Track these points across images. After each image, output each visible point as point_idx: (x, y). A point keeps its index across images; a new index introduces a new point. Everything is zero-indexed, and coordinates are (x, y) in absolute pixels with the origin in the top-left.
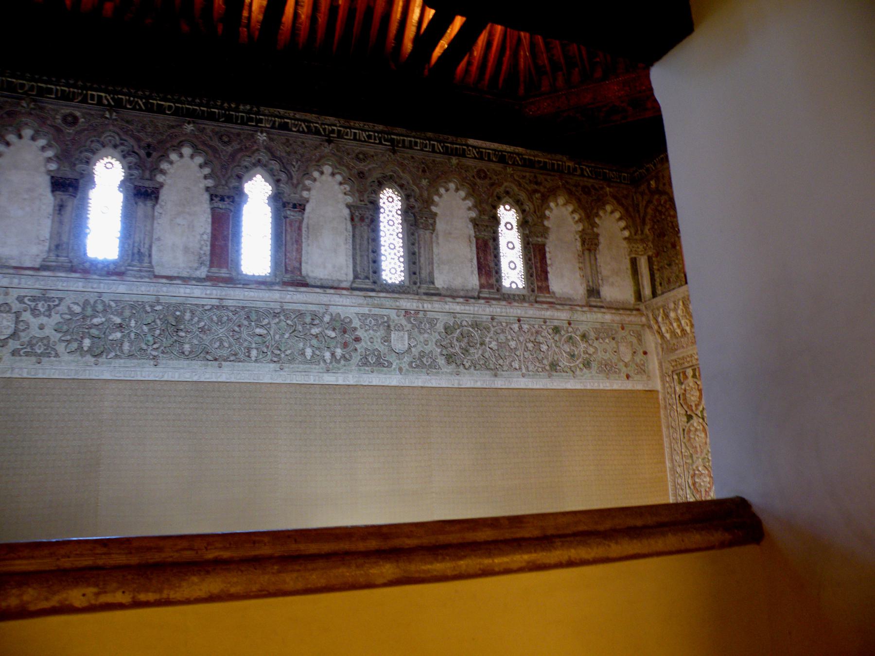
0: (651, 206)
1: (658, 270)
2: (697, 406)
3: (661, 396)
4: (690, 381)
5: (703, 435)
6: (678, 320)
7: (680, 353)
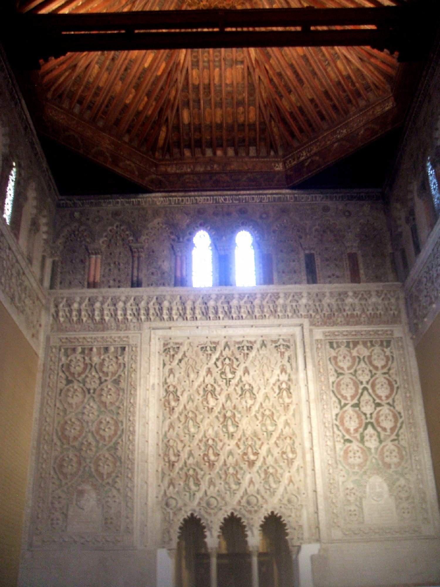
0: (69, 228)
1: (61, 273)
2: (79, 375)
3: (41, 362)
4: (79, 357)
5: (81, 396)
6: (79, 311)
7: (71, 335)
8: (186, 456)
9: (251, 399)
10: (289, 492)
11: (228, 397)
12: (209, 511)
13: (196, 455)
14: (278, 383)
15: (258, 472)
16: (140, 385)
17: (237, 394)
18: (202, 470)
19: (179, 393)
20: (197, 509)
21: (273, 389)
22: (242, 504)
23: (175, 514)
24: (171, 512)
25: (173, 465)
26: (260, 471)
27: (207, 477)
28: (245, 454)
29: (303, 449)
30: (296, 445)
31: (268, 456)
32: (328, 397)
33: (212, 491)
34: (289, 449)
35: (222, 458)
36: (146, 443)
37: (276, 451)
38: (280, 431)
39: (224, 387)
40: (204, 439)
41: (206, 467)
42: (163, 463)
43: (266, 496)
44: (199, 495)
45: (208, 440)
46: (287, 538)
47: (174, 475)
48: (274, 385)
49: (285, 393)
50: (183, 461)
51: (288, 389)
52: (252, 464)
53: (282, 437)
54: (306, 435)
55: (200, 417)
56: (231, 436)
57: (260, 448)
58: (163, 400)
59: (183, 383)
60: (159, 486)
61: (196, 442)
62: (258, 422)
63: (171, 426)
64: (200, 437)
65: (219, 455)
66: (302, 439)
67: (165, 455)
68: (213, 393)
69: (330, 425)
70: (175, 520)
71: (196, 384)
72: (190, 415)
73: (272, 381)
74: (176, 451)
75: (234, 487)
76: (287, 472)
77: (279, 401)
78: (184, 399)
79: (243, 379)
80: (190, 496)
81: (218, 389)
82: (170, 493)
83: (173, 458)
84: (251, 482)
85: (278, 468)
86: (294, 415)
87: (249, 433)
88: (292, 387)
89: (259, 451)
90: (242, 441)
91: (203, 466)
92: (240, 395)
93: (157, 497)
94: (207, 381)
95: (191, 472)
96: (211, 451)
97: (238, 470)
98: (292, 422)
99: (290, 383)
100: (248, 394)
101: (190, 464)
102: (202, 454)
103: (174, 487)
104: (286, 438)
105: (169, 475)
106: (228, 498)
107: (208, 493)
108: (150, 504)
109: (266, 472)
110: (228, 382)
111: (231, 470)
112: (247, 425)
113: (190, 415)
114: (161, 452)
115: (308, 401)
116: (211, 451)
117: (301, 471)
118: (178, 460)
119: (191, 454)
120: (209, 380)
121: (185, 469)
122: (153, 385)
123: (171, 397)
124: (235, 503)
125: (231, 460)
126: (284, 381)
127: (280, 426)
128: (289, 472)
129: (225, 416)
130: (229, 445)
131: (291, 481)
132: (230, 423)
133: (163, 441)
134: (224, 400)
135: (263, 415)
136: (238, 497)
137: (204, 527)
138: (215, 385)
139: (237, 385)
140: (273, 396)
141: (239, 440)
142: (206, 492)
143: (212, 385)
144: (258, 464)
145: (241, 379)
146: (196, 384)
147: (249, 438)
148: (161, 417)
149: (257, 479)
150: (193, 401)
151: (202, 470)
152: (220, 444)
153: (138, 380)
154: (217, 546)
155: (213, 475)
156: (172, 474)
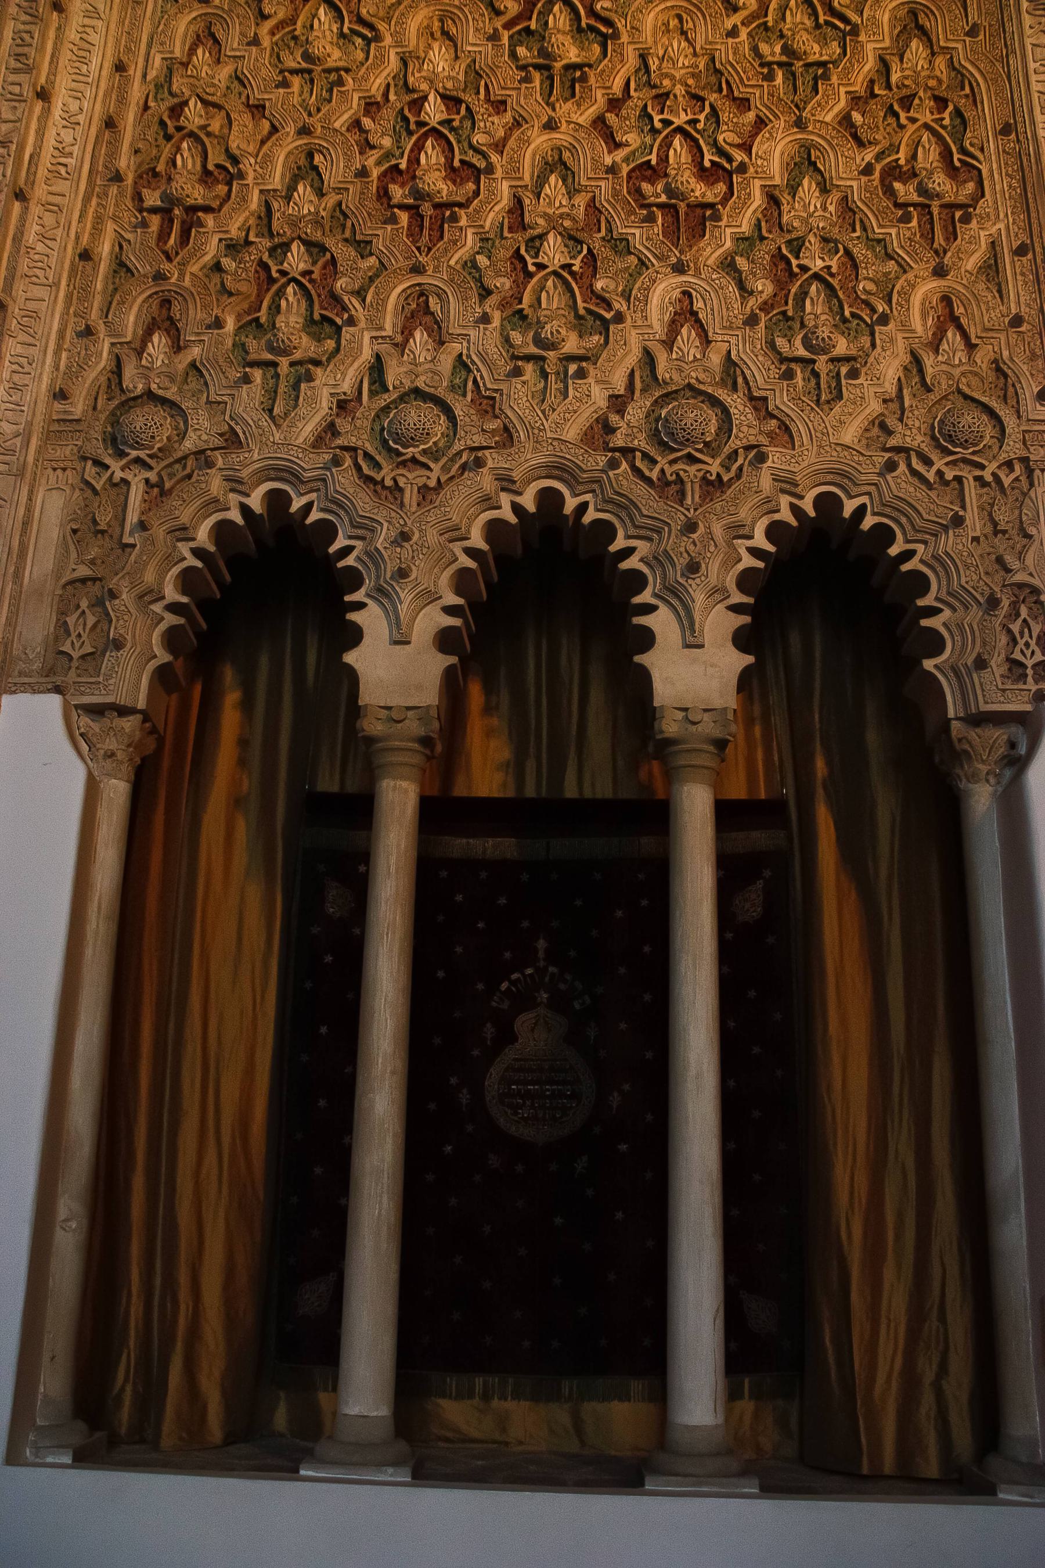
8: (277, 181)
12: (387, 474)
13: (335, 170)
15: (728, 265)
18: (363, 247)
20: (311, 464)
22: (619, 440)
23: (159, 492)
24: (137, 480)
26: (741, 262)
31: (793, 188)
33: (422, 361)
34: (929, 157)
36: (39, 106)
41: (389, 239)
42: (129, 217)
43: (781, 400)
45: (418, 104)
46: (928, 664)
47: (187, 274)
50: (255, 200)
52: (689, 221)
60: (88, 332)
64: (376, 86)
65: (476, 173)
67: (150, 175)
70: (159, 532)
74: (216, 156)
76: (921, 268)
80: (272, 394)
82: (146, 373)
84: (686, 312)
85: (859, 251)
89: (739, 156)
90: (631, 110)
93: (61, 395)
95: (296, 260)
96: (432, 155)
97: (602, 251)
101: (294, 222)
103: (177, 347)
104: (907, 102)
105: (159, 277)
106: (519, 398)
107: (394, 374)
109: (783, 269)
111: (554, 252)
114: (125, 162)
116: (432, 155)
119: (306, 169)
124: (572, 432)
127: (871, 47)
128: (940, 272)
130: (550, 126)
133: (146, 107)
137: (354, 579)
141: (614, 104)
142: (377, 369)
147: (679, 90)
149: (719, 301)
151: (363, 247)
154: (430, 696)
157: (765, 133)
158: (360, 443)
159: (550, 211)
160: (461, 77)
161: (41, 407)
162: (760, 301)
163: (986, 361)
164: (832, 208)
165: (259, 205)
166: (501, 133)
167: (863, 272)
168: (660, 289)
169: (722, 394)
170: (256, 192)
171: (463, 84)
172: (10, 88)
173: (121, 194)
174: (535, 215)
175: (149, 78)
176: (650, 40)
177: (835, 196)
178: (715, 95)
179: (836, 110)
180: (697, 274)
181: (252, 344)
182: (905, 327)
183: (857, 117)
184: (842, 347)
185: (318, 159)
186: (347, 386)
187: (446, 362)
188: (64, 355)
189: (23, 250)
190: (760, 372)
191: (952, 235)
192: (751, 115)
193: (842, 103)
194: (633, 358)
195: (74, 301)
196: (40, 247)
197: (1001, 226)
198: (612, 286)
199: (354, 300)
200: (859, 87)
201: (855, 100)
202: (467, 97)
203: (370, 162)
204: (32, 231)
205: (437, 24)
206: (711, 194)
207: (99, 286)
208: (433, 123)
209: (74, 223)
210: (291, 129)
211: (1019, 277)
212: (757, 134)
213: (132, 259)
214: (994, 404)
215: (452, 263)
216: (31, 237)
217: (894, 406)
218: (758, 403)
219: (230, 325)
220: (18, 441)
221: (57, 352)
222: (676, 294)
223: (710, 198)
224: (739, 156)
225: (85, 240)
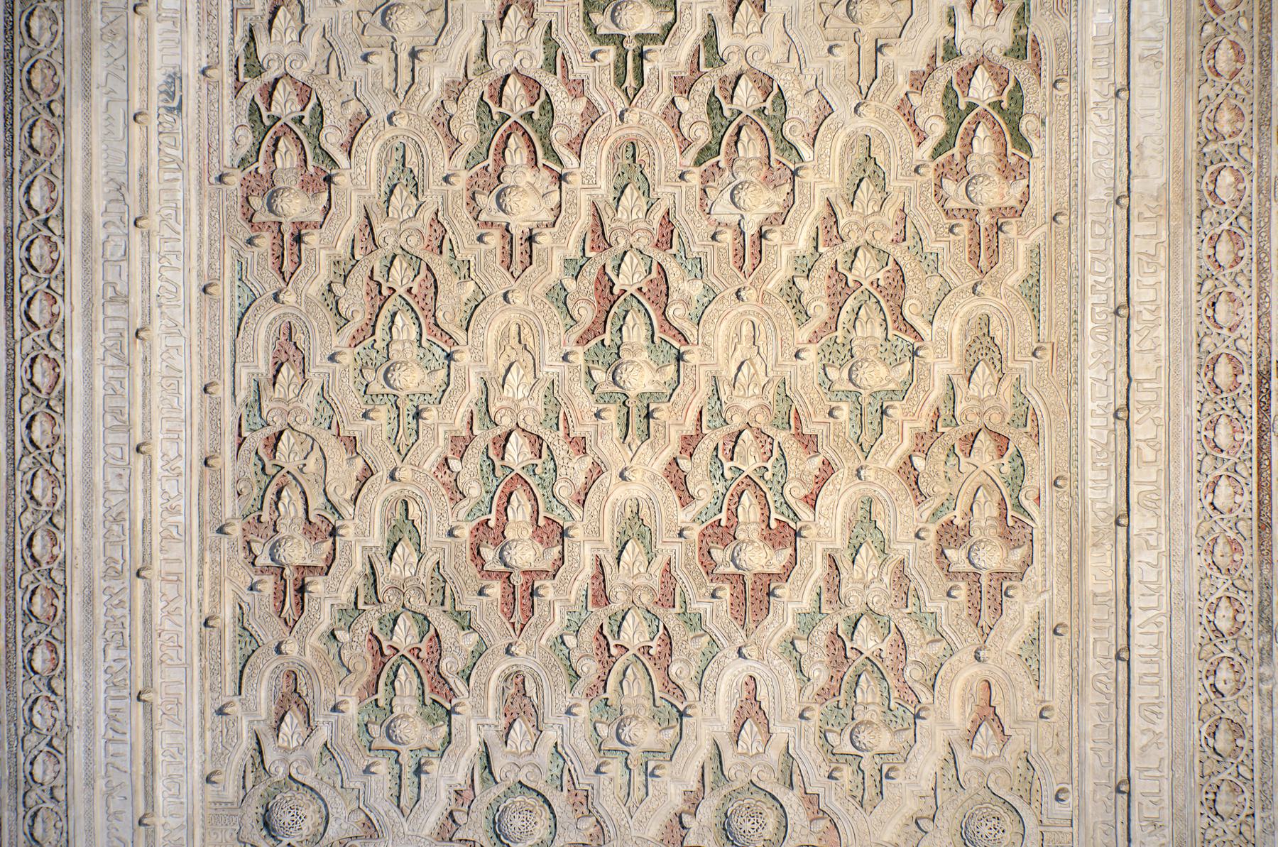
8: (377, 539)
9: (770, 182)
10: (973, 783)
11: (631, 164)
13: (433, 534)
14: (946, 72)
16: (87, 96)
17: (685, 144)
19: (332, 139)
21: (911, 118)
25: (301, 589)
27: (496, 669)
28: (722, 532)
29: (1074, 515)
30: (1037, 479)
32: (1251, 186)
34: (987, 511)
35: (583, 553)
36: (139, 462)
37: (904, 522)
38: (938, 391)
39: (606, 94)
40: (483, 437)
41: (487, 606)
42: (245, 577)
43: (833, 801)
44: (447, 775)
47: (304, 648)
48: (919, 82)
49: (984, 144)
50: (359, 565)
51: (1010, 112)
52: (756, 596)
53: (953, 435)
54: (1096, 427)
55: (454, 296)
56: (641, 418)
57: (811, 501)
58: (235, 179)
59: (355, 71)
61: (432, 450)
62: (804, 334)
63: (289, 351)
66: (1073, 453)
68: (537, 132)
69: (1249, 379)
71: (437, 74)
72: (400, 276)
73: (907, 57)
75: (644, 735)
77: (942, 199)
78: (361, 177)
79: (724, 41)
81: (568, 109)
83: (297, 552)
84: (751, 709)
85: (908, 628)
86: (1032, 290)
87: (746, 402)
88: (1036, 98)
89: (804, 512)
90: (704, 450)
91: (469, 601)
92: (707, 152)
94: (500, 60)
95: (405, 635)
96: (520, 511)
98: (1015, 335)
99: (1020, 71)
100: (751, 147)
101: (398, 589)
102: (465, 532)
106: (608, 803)
108: (166, 818)
110: (631, 64)
111: (635, 633)
112: (742, 347)
113: (400, 276)
114: (230, 508)
115: (1123, 199)
117: (1054, 649)
118: (332, 557)
119: (402, 528)
120: (518, 49)
121: (372, 616)
122: (174, 79)
123: (287, 158)
125: (635, 573)
126: (981, 60)
127: (941, 364)
129: (607, 292)
131: (988, 714)
132: (635, 332)
133: (242, 440)
134: (604, 188)
135: (841, 287)
136: (671, 790)
138: (551, 84)
139: (685, 86)
140: (903, 154)
141: (689, 445)
143: (532, 84)
144: (795, 599)
145: (710, 39)
146: (437, 74)
148: (226, 290)
149: (782, 693)
150: (416, 189)
152: (576, 470)
153: (74, 54)
155: (524, 659)
156: (291, 648)
157: (828, 488)
158: (476, 838)
159: (629, 582)
160: (541, 408)
161: (198, 797)
162: (816, 689)
163: (1015, 755)
164: (886, 580)
165: (364, 564)
166: (580, 481)
167: (911, 658)
168: (727, 677)
169: (779, 792)
170: (358, 550)
171: (543, 417)
172: (110, 450)
173: (233, 546)
174: (615, 581)
175: (239, 400)
176: (722, 358)
177: (890, 566)
178: (783, 434)
179: (899, 452)
180: (761, 659)
181: (375, 730)
182: (945, 720)
183: (919, 462)
184: (884, 740)
185: (414, 511)
186: (461, 778)
187: (545, 751)
188: (208, 734)
189: (155, 635)
190: (812, 766)
191: (999, 610)
192: (817, 461)
193: (907, 445)
194: (705, 750)
195: (208, 674)
196: (167, 625)
197: (1046, 596)
198: (685, 673)
199: (459, 683)
200: (924, 424)
201: (920, 436)
202: (548, 437)
203: (462, 515)
204: (159, 604)
205: (514, 329)
206: (778, 560)
207: (228, 657)
208: (518, 470)
209: (195, 591)
210: (383, 473)
211: (1057, 659)
212: (825, 480)
213: (254, 626)
214: (1017, 804)
215: (543, 641)
216: (157, 619)
217: (931, 801)
218: (812, 800)
219: (352, 707)
220: (183, 834)
221: (202, 736)
222: (744, 677)
223: (776, 568)
224: (804, 512)
225: (207, 611)
